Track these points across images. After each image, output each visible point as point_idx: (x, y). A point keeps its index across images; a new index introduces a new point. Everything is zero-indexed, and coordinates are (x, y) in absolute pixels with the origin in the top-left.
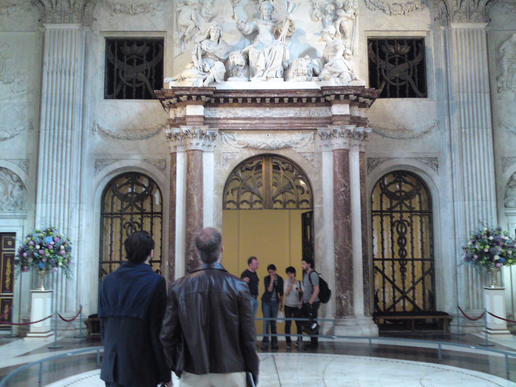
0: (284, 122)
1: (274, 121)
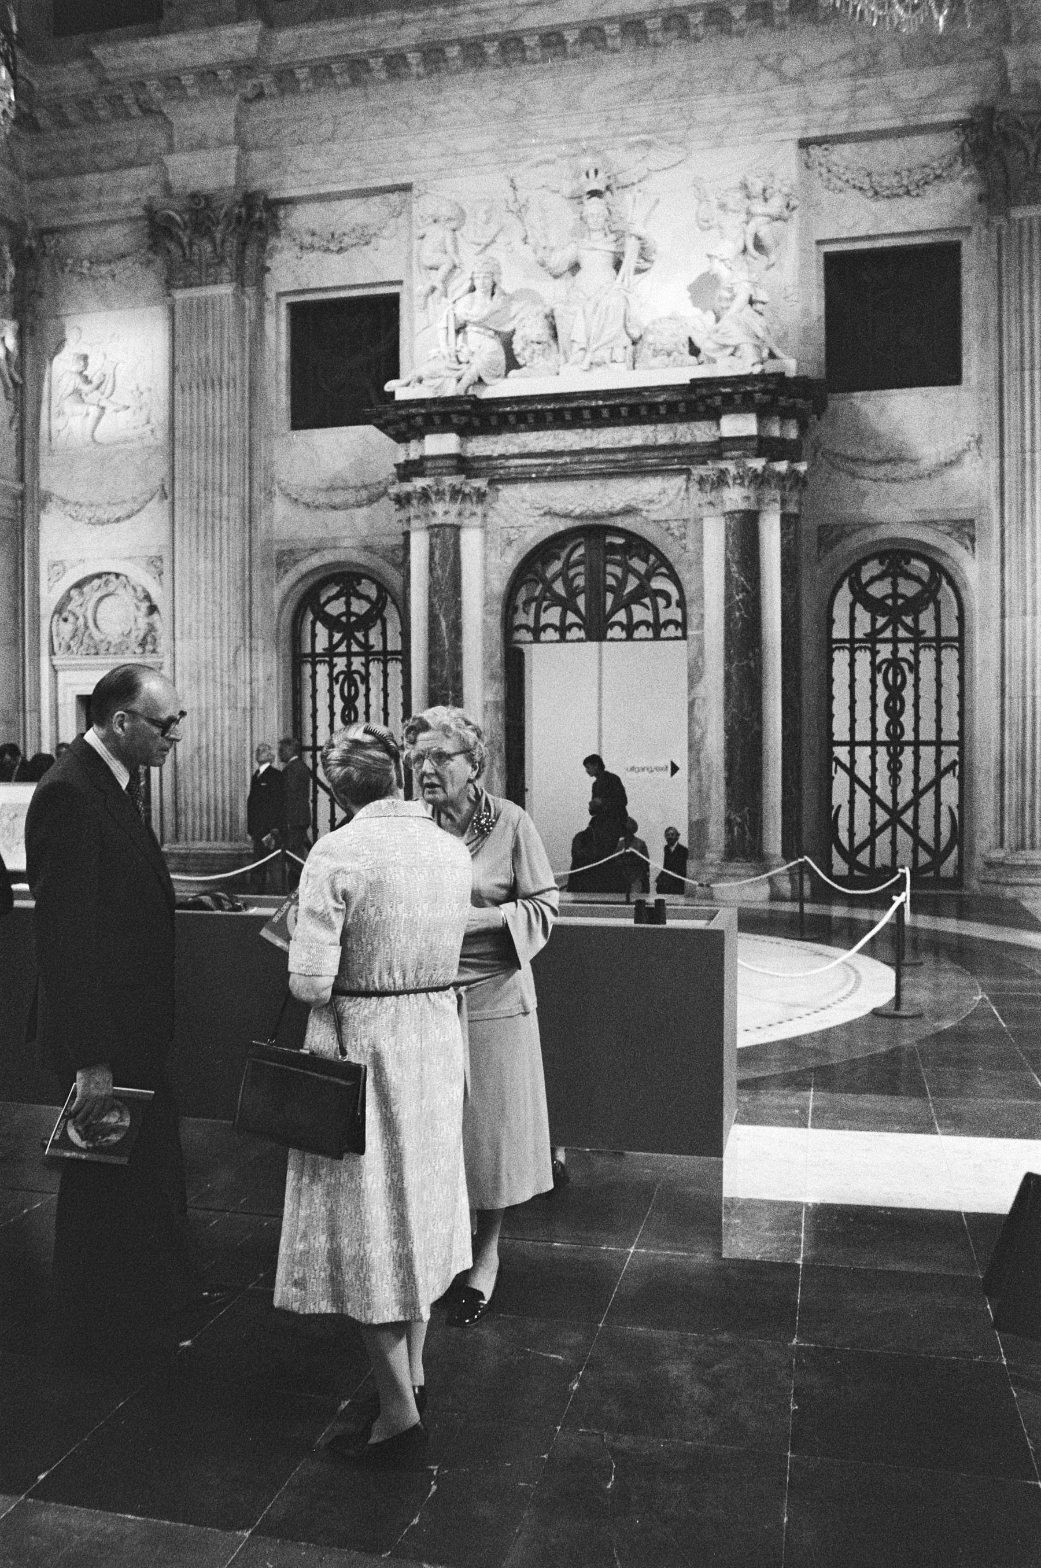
0: (621, 456)
1: (601, 457)
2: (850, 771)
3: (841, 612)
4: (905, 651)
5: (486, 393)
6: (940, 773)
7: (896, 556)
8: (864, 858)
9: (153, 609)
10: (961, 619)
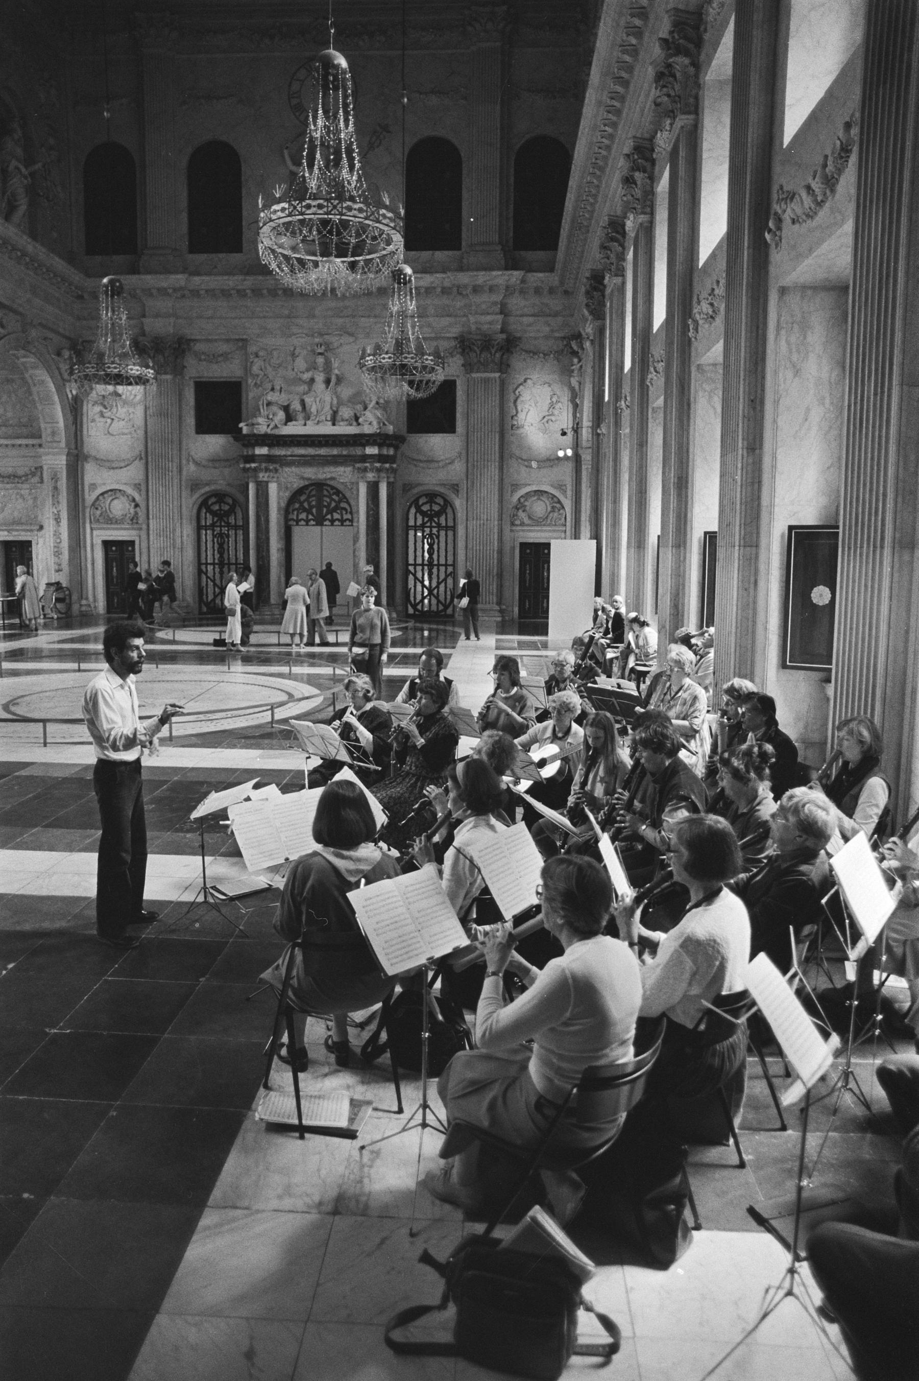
2: (414, 575)
3: (411, 516)
4: (435, 531)
6: (447, 576)
7: (431, 497)
8: (419, 607)
9: (137, 506)
10: (454, 519)
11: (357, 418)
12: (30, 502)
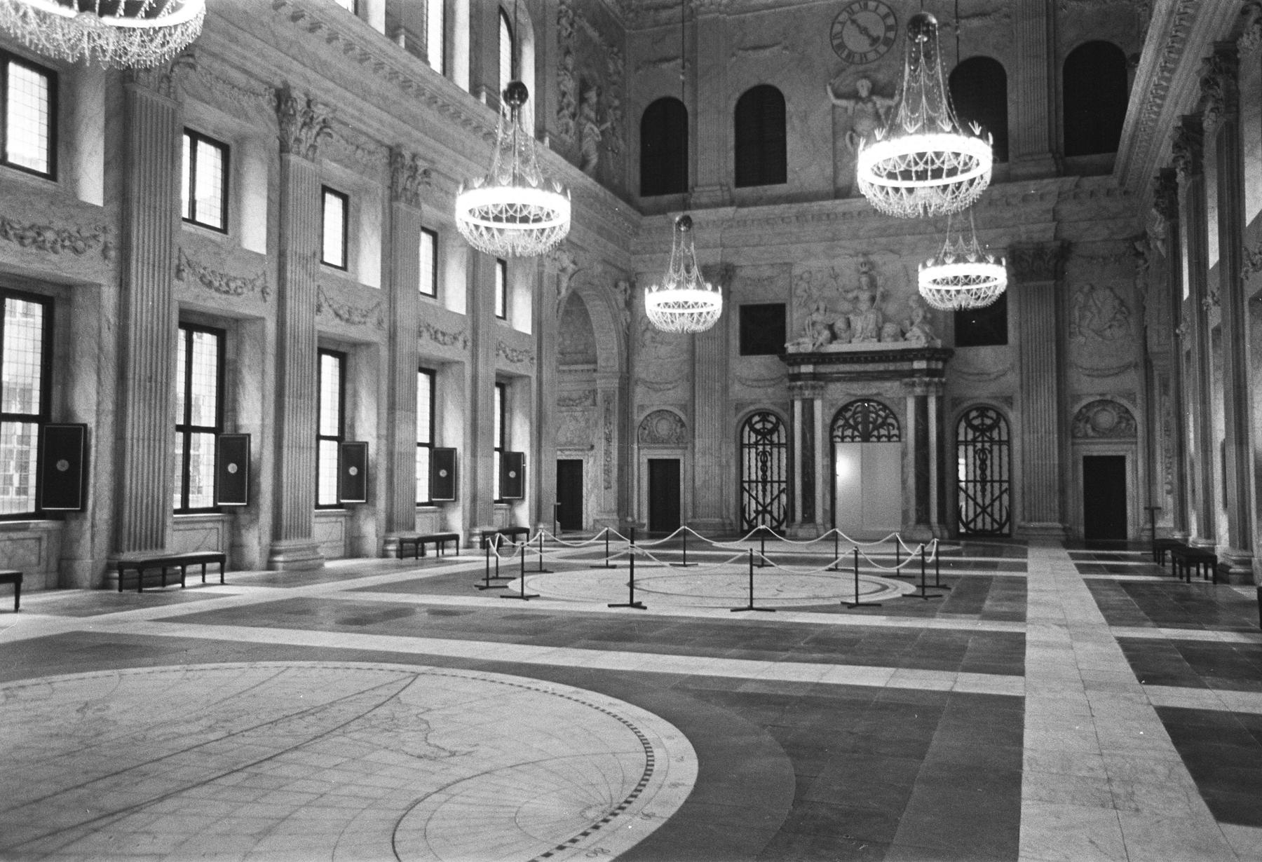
2: (966, 492)
3: (962, 431)
4: (987, 445)
5: (823, 350)
6: (1001, 493)
7: (983, 410)
8: (972, 526)
10: (1009, 434)
11: (903, 334)
12: (583, 424)
